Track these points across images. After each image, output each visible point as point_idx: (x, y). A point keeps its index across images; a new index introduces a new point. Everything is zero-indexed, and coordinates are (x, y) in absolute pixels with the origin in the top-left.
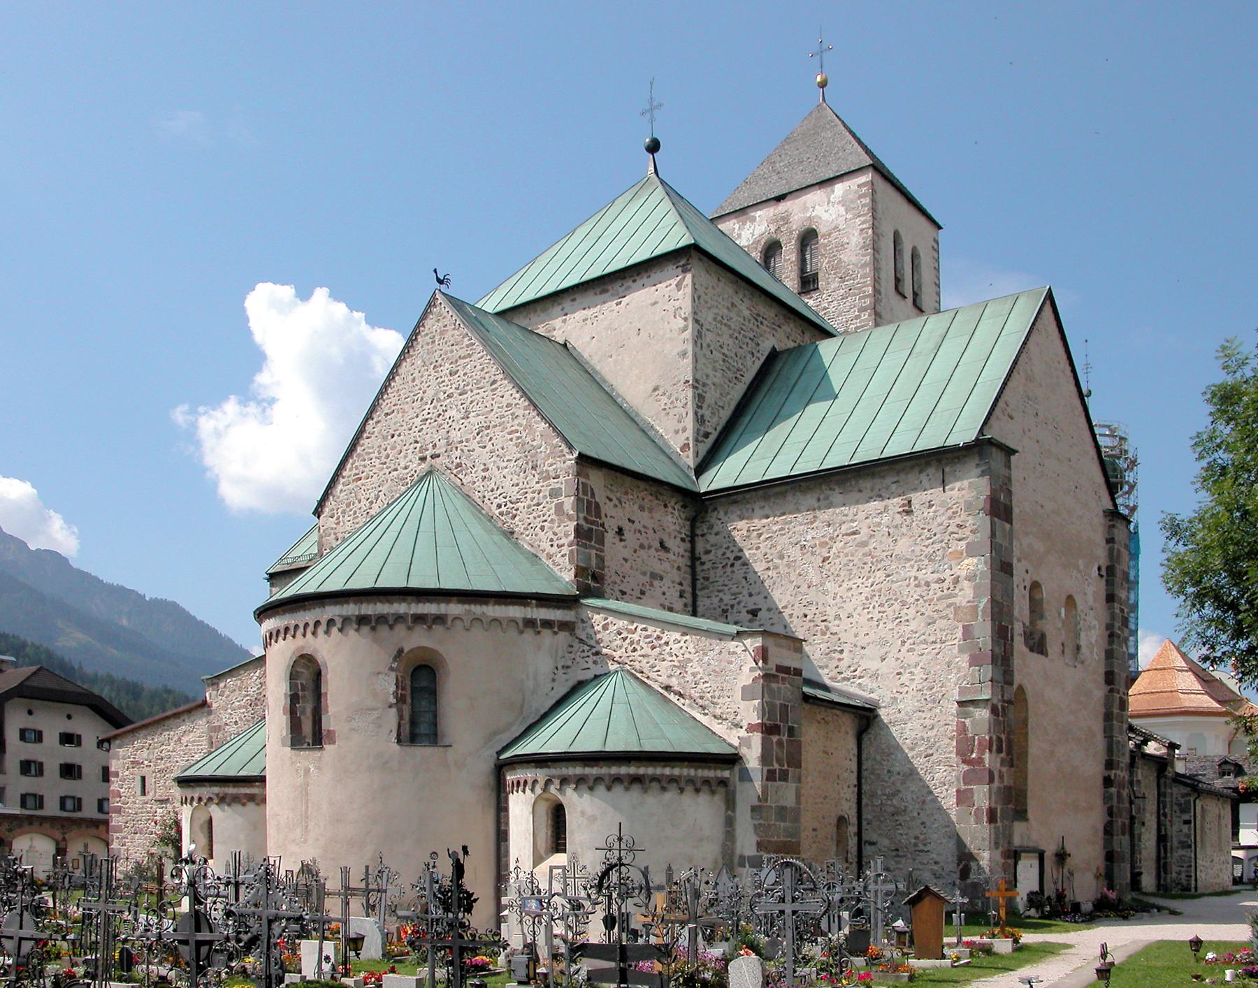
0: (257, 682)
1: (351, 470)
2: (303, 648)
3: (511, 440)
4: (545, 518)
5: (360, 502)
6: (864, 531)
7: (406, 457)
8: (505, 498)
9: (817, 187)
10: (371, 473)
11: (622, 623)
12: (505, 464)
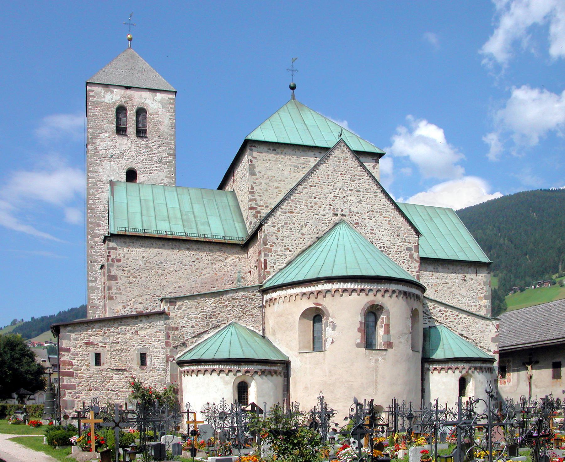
0: (212, 305)
1: (287, 206)
2: (375, 301)
3: (386, 220)
4: (404, 258)
5: (294, 224)
6: (450, 283)
7: (324, 210)
8: (384, 245)
9: (148, 90)
10: (301, 212)
11: (442, 308)
12: (383, 230)
